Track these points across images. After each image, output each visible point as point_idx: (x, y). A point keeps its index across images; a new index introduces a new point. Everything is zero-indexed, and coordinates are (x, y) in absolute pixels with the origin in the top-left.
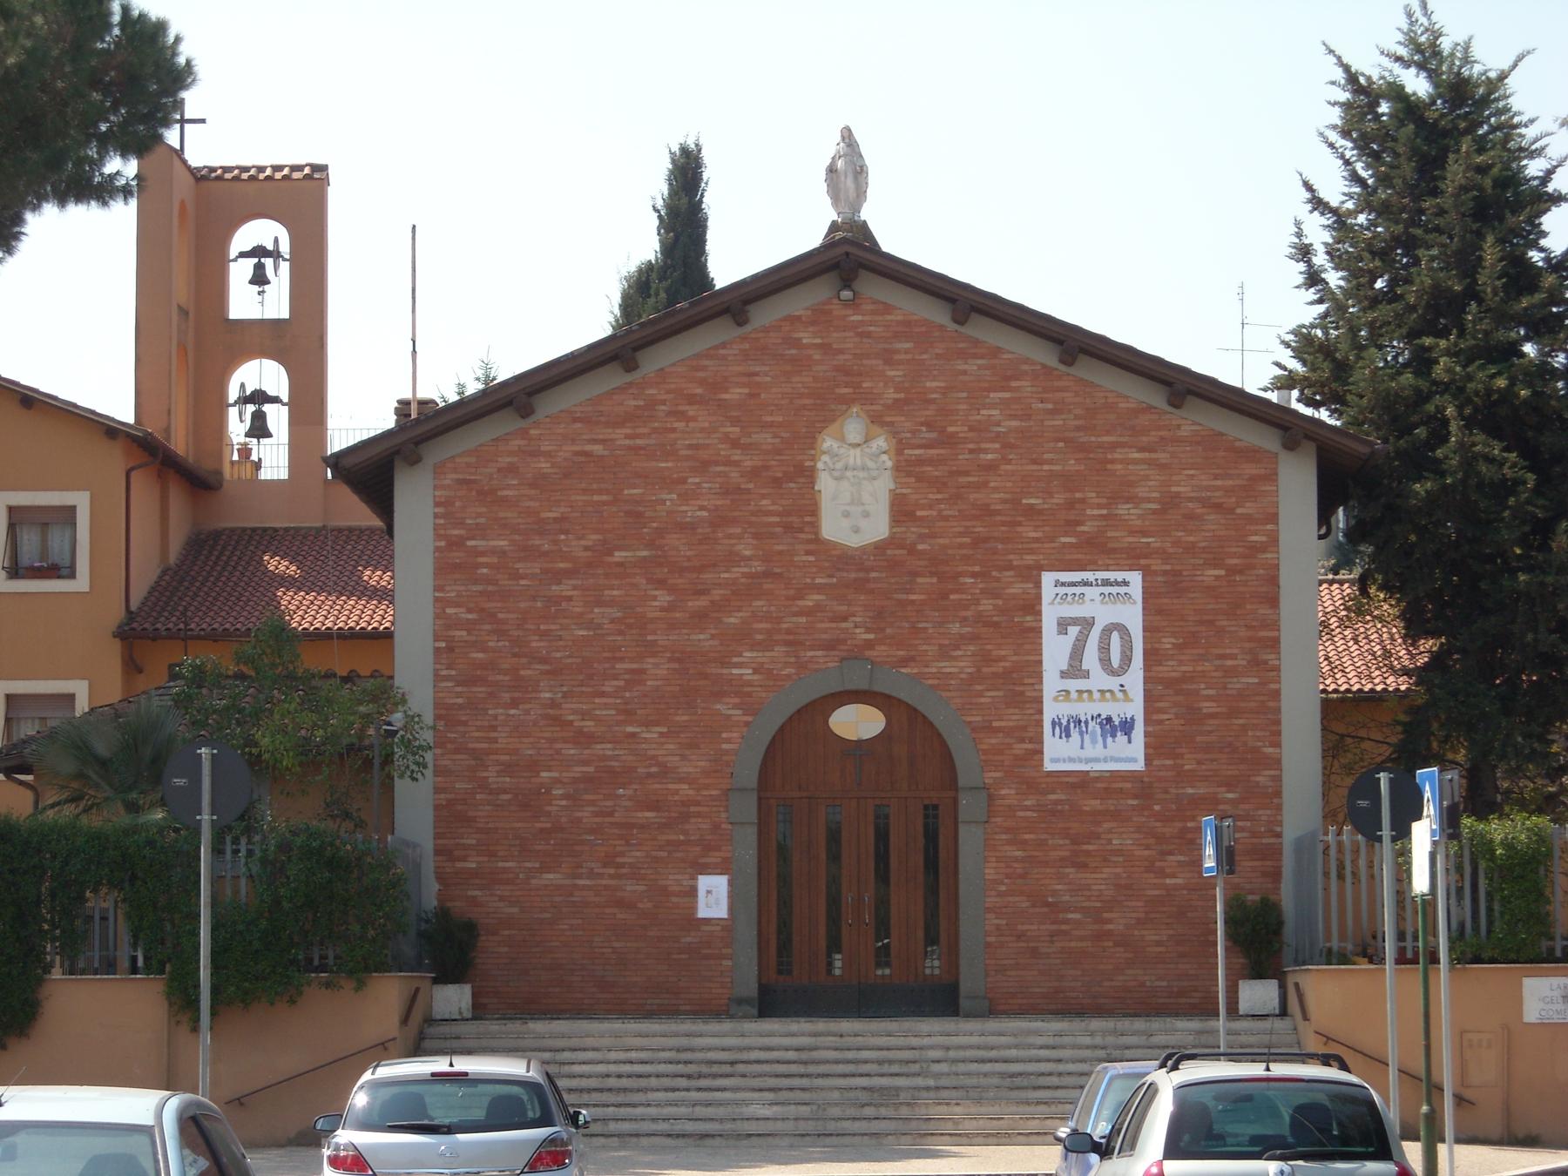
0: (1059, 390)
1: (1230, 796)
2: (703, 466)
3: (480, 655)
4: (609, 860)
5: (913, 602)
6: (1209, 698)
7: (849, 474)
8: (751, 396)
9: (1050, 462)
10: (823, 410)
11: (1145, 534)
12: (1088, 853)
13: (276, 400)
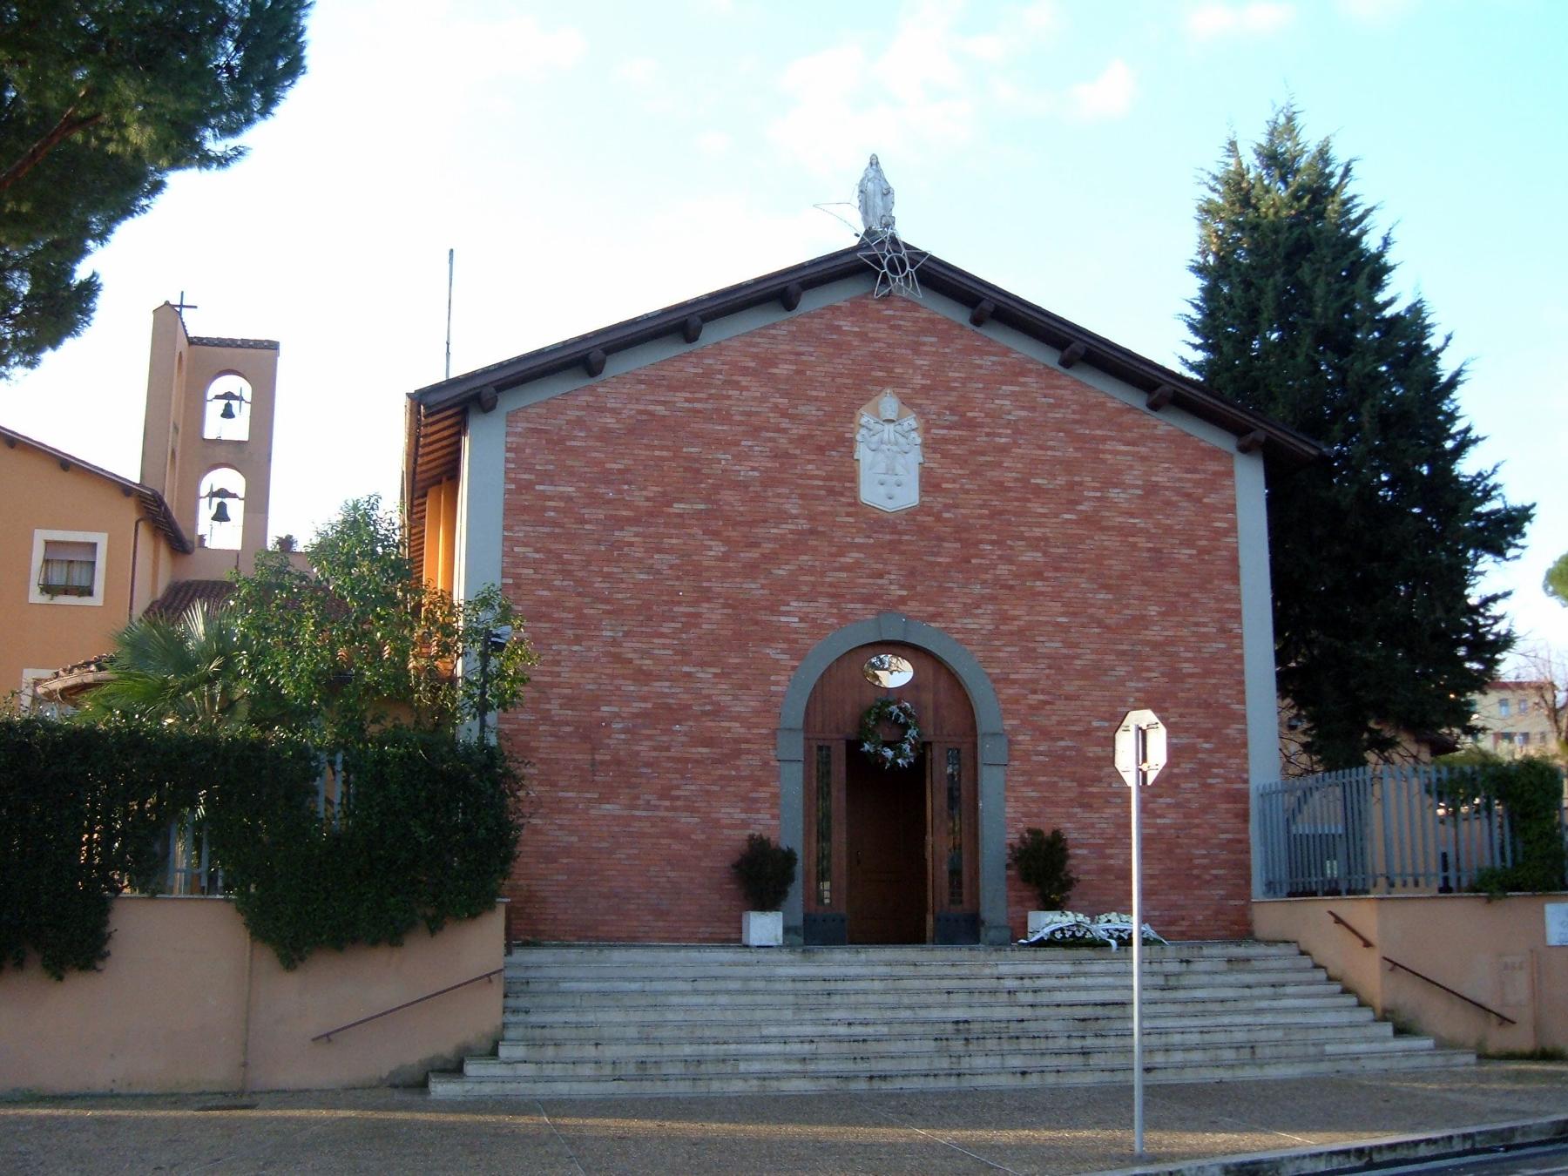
0: (1058, 387)
1: (1206, 746)
2: (755, 432)
3: (545, 593)
4: (664, 794)
5: (939, 564)
6: (1187, 660)
7: (884, 447)
8: (798, 372)
9: (1052, 448)
10: (861, 389)
11: (1132, 515)
12: (1092, 795)
13: (234, 496)
